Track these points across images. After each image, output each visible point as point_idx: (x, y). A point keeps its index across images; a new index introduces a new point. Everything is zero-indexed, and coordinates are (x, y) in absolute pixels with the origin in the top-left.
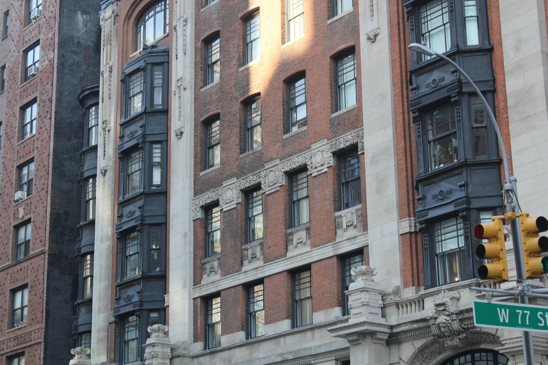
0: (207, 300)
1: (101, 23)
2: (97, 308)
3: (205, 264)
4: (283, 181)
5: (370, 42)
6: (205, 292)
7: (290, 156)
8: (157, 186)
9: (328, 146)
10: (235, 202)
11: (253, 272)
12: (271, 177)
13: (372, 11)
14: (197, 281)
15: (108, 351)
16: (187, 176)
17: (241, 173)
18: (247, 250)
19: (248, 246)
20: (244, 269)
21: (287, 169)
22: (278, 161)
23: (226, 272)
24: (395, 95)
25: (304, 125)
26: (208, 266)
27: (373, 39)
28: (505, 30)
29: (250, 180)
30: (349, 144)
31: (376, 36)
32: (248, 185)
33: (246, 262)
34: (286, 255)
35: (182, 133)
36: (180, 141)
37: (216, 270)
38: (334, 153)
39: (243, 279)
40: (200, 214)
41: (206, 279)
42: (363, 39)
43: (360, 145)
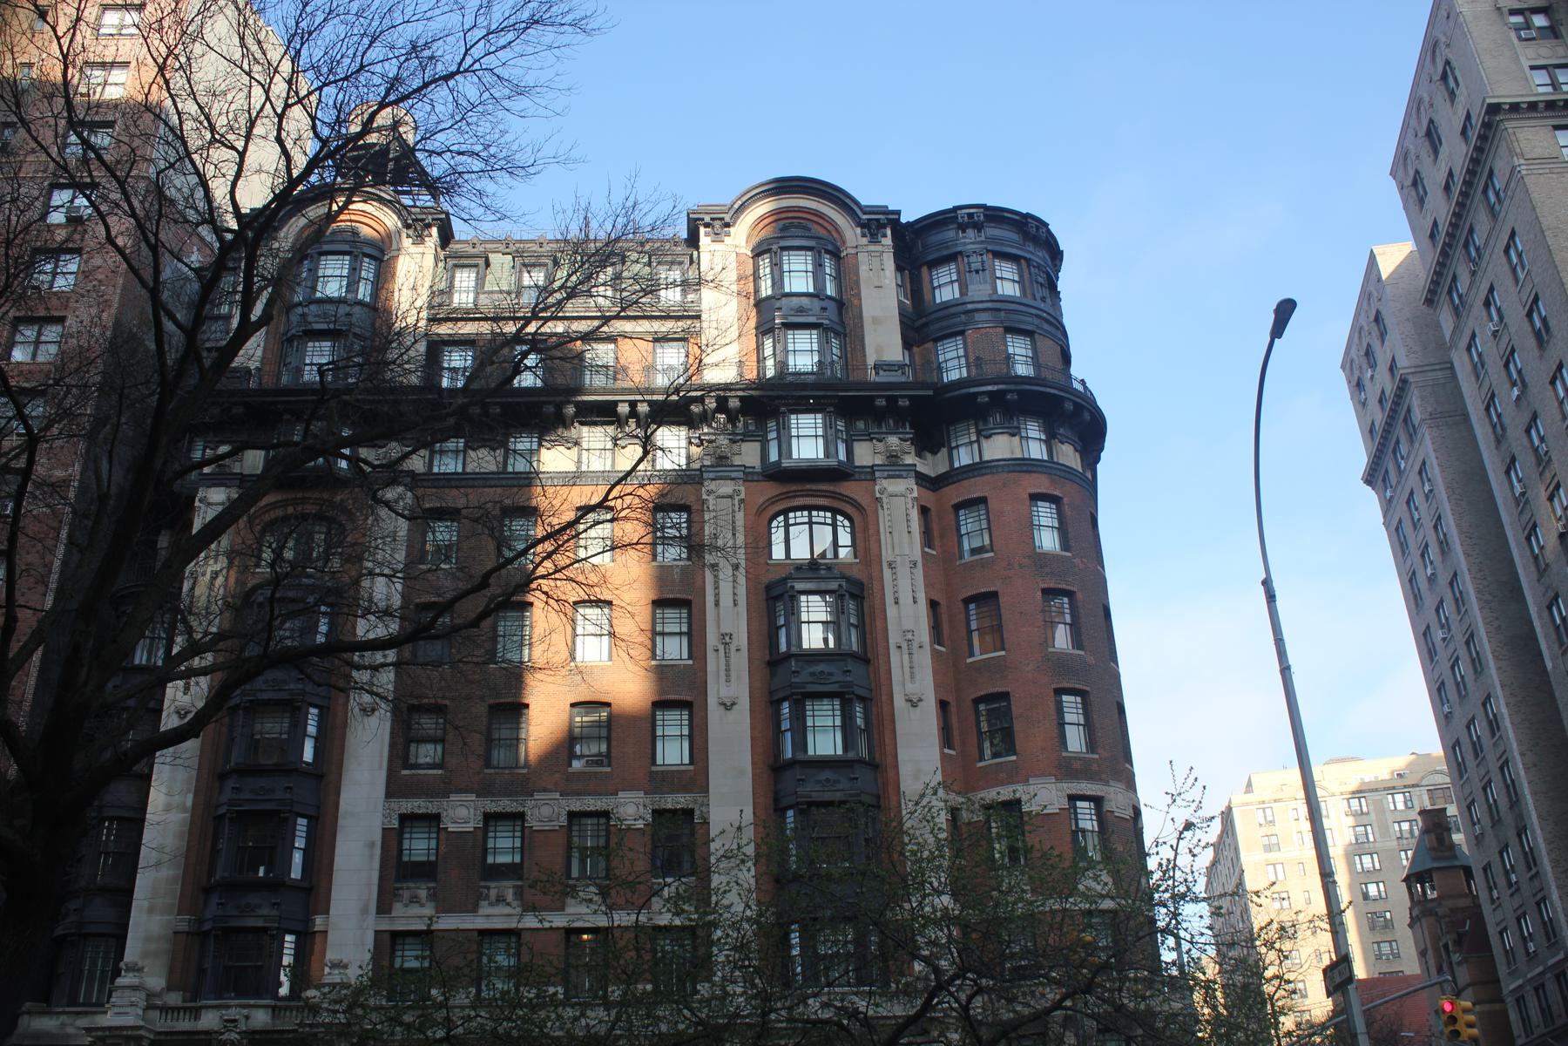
0: (396, 938)
1: (197, 503)
2: (146, 904)
3: (398, 889)
4: (563, 820)
5: (722, 708)
6: (400, 926)
7: (579, 794)
8: (307, 763)
9: (648, 801)
10: (471, 825)
11: (503, 919)
12: (546, 811)
13: (728, 675)
14: (383, 908)
15: (171, 971)
16: (380, 768)
17: (484, 791)
18: (488, 888)
19: (492, 885)
20: (482, 911)
21: (573, 808)
22: (557, 795)
23: (445, 907)
24: (754, 775)
25: (599, 763)
26: (406, 894)
27: (728, 706)
28: (903, 755)
29: (505, 805)
30: (679, 806)
31: (733, 704)
32: (499, 809)
33: (484, 903)
34: (563, 910)
35: (373, 710)
36: (366, 719)
37: (423, 901)
38: (654, 811)
39: (479, 923)
40: (395, 824)
41: (398, 909)
42: (712, 701)
43: (697, 813)
